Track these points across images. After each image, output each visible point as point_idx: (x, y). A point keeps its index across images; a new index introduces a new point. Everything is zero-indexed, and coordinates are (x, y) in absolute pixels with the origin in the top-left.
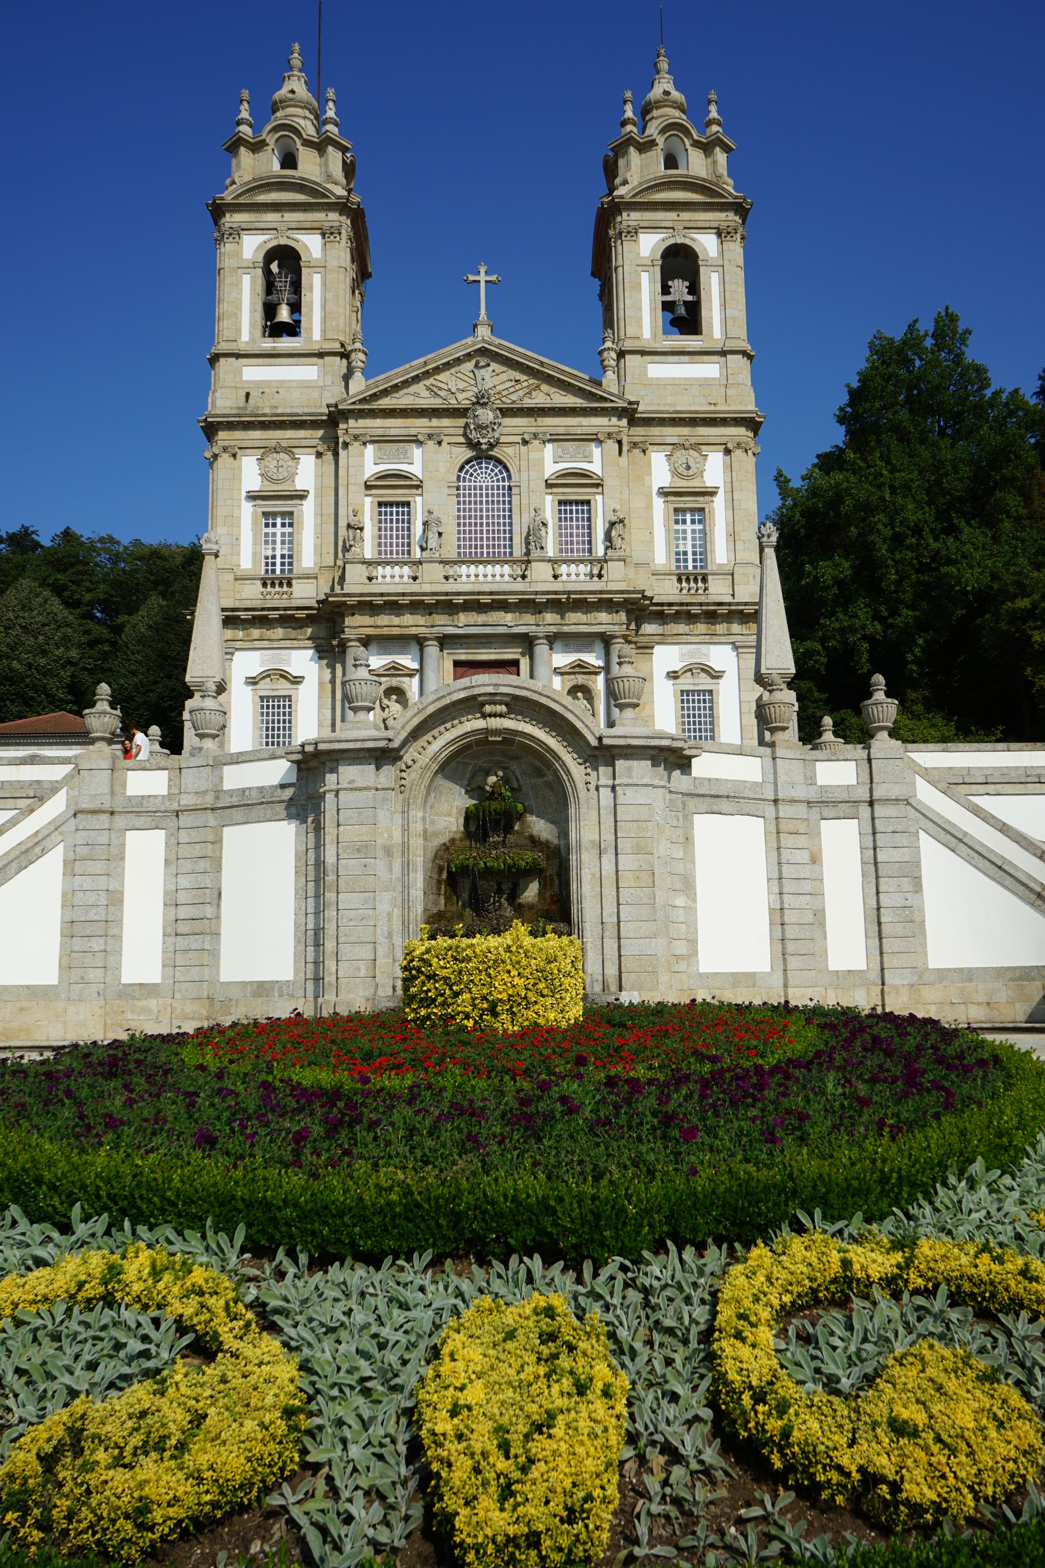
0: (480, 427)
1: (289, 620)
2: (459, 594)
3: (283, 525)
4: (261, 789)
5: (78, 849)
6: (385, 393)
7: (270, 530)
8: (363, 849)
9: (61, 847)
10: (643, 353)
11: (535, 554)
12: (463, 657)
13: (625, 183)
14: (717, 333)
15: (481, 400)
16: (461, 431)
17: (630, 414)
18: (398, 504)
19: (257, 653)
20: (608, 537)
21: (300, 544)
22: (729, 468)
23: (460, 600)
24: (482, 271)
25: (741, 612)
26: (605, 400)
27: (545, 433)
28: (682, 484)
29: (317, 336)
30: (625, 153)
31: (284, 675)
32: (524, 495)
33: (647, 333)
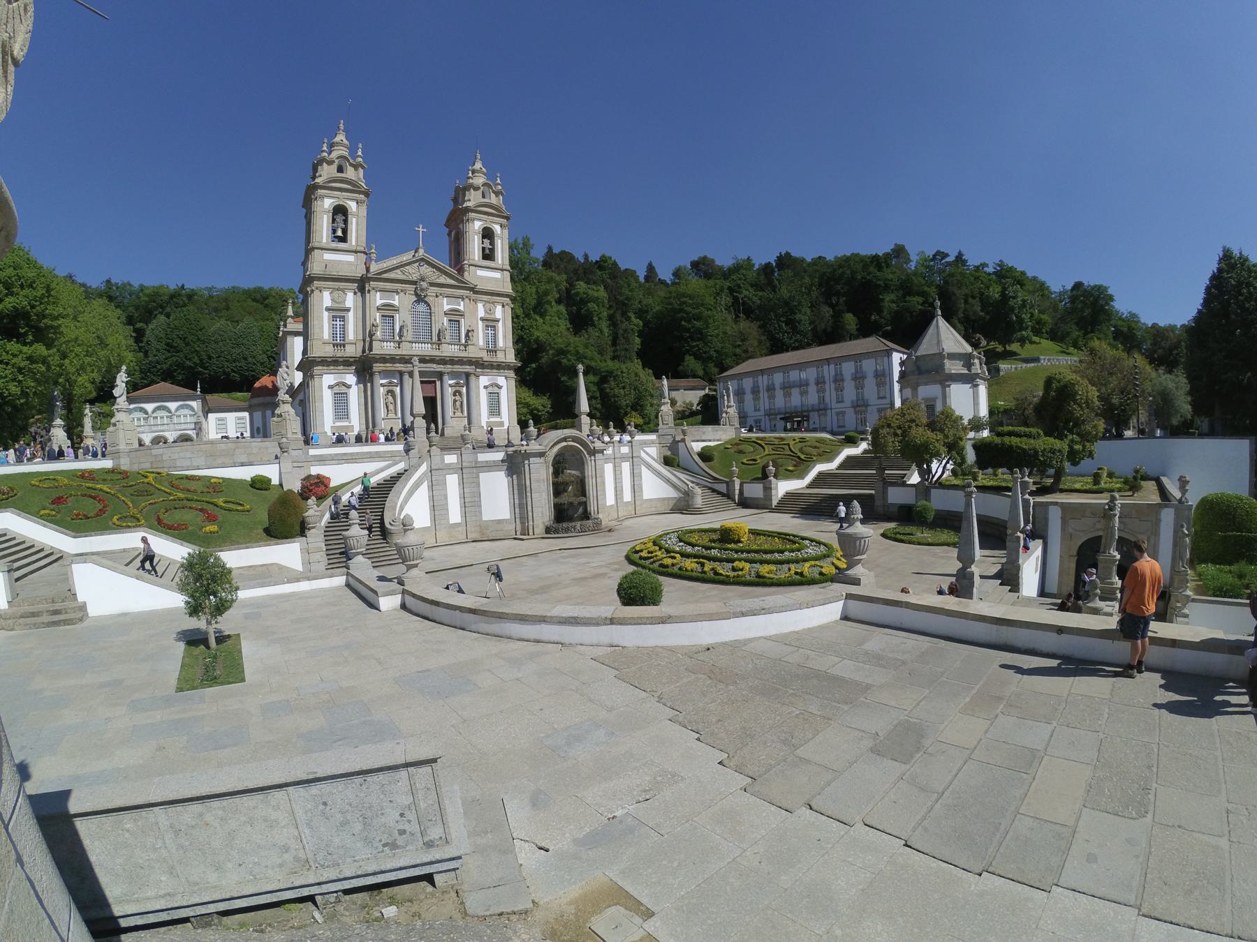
0: (422, 290)
1: (346, 362)
6: (385, 272)
7: (335, 323)
8: (538, 481)
10: (476, 266)
11: (443, 341)
13: (469, 200)
15: (423, 279)
17: (473, 290)
19: (332, 375)
20: (467, 335)
22: (504, 312)
24: (421, 226)
28: (488, 316)
29: (354, 243)
30: (469, 190)
31: (344, 384)
33: (476, 259)
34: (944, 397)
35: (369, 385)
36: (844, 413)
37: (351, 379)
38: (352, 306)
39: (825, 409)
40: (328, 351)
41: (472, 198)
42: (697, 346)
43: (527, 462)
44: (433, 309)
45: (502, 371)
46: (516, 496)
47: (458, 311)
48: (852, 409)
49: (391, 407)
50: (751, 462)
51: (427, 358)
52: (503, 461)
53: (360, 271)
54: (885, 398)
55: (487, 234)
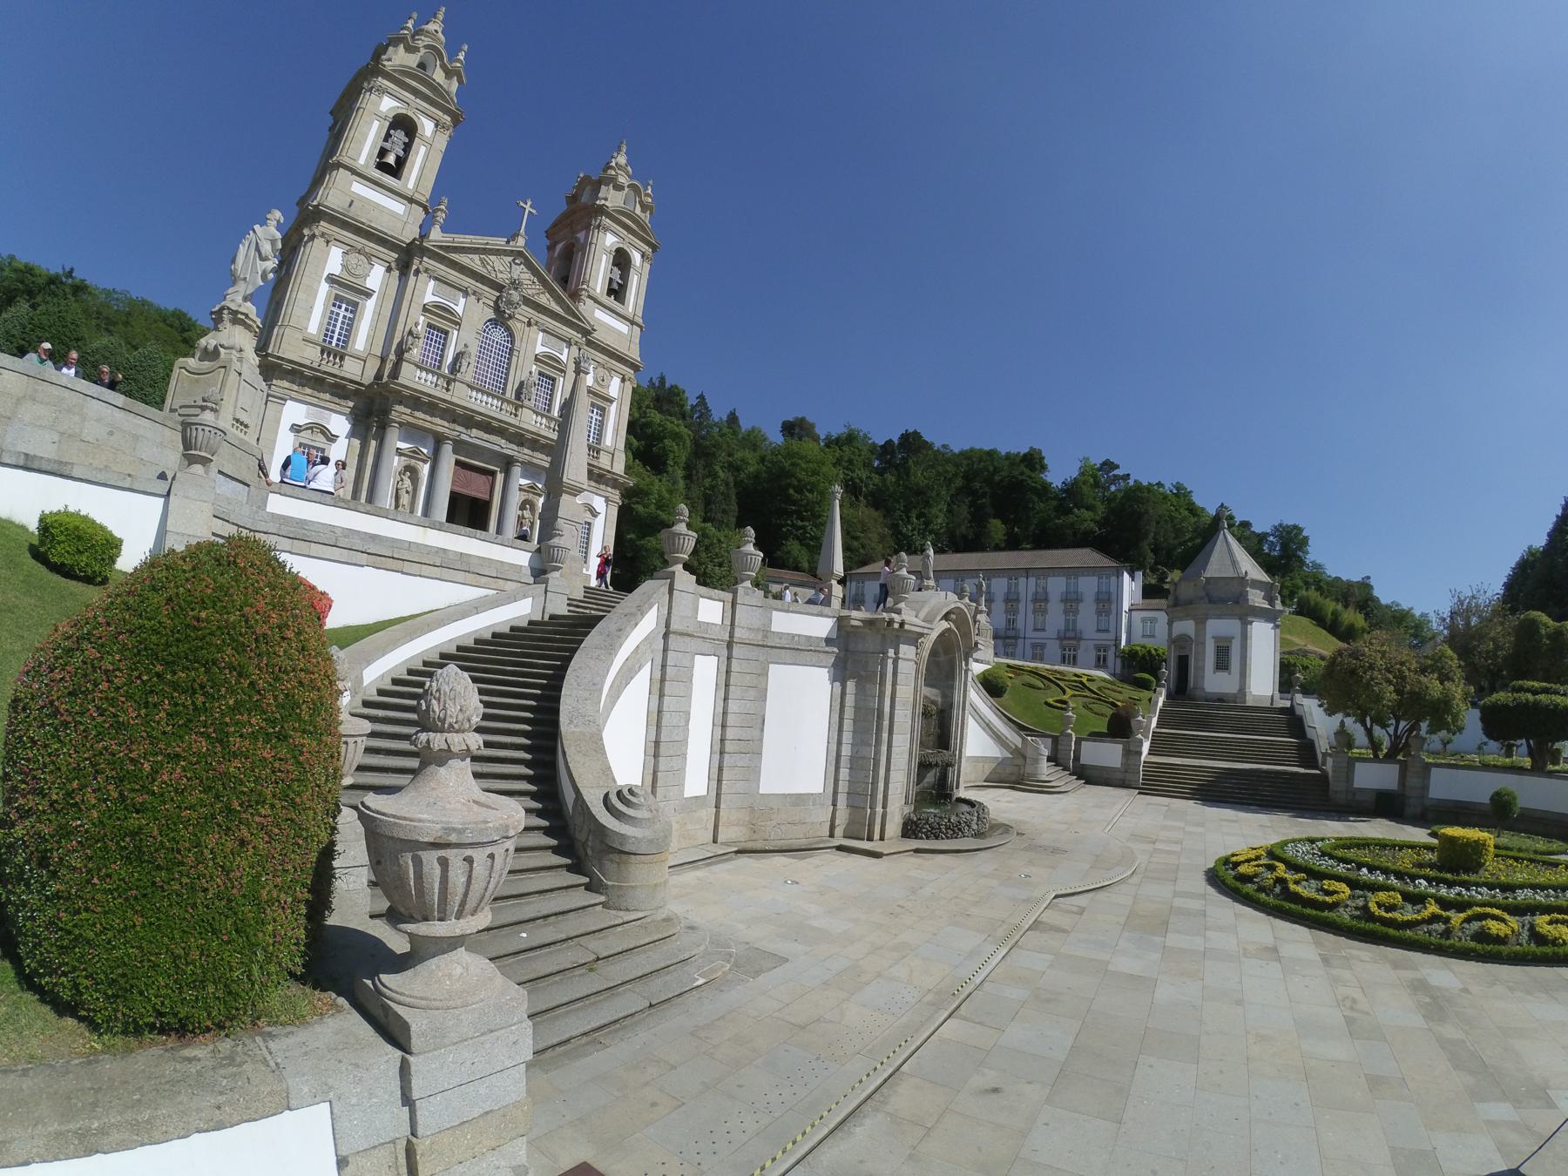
0: (510, 303)
1: (339, 389)
2: (481, 414)
3: (346, 310)
4: (809, 638)
5: (669, 669)
7: (336, 310)
9: (647, 669)
10: (596, 301)
12: (463, 458)
14: (630, 310)
16: (494, 298)
17: (586, 333)
18: (439, 330)
21: (357, 330)
22: (622, 390)
23: (479, 418)
24: (529, 203)
25: (616, 480)
26: (580, 320)
27: (543, 324)
31: (324, 431)
32: (521, 359)
33: (598, 290)
34: (1245, 637)
35: (373, 443)
36: (1043, 646)
37: (339, 424)
38: (377, 290)
39: (1016, 638)
40: (311, 355)
41: (609, 197)
42: (803, 528)
43: (891, 653)
44: (517, 343)
45: (603, 487)
46: (847, 737)
47: (557, 361)
48: (1058, 642)
49: (405, 499)
50: (1059, 705)
51: (495, 424)
52: (828, 641)
53: (409, 234)
54: (1107, 631)
55: (621, 260)
